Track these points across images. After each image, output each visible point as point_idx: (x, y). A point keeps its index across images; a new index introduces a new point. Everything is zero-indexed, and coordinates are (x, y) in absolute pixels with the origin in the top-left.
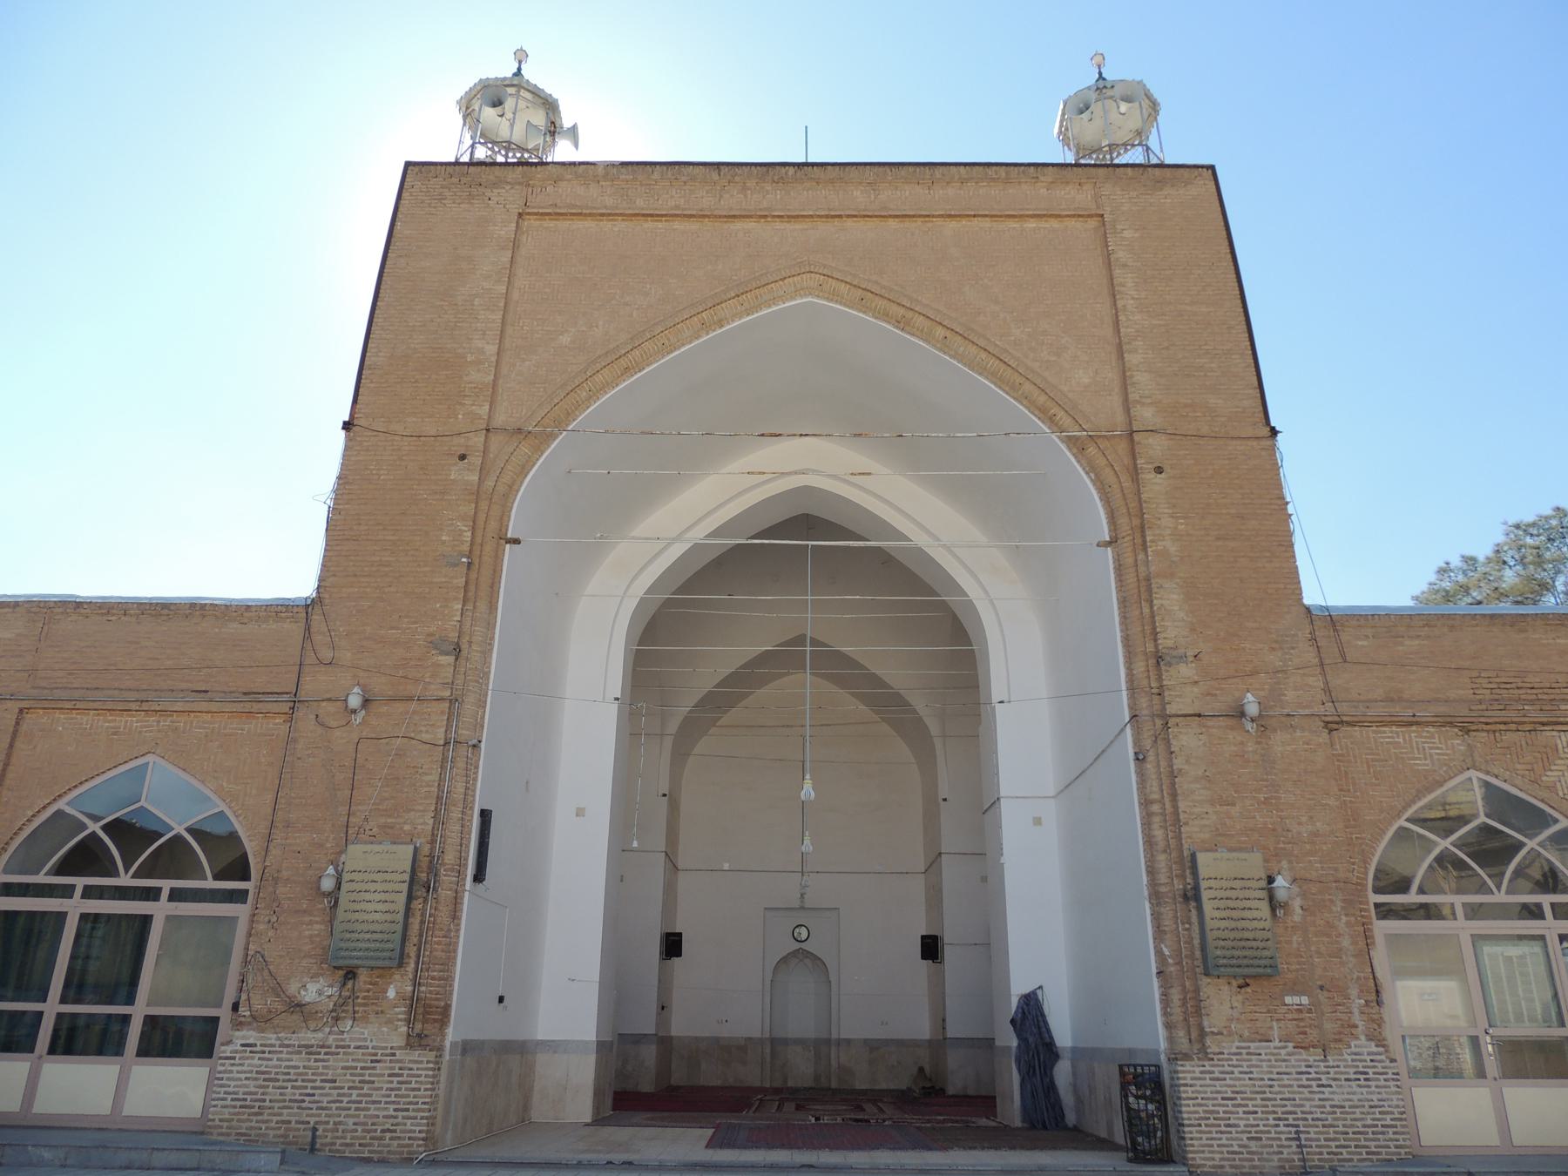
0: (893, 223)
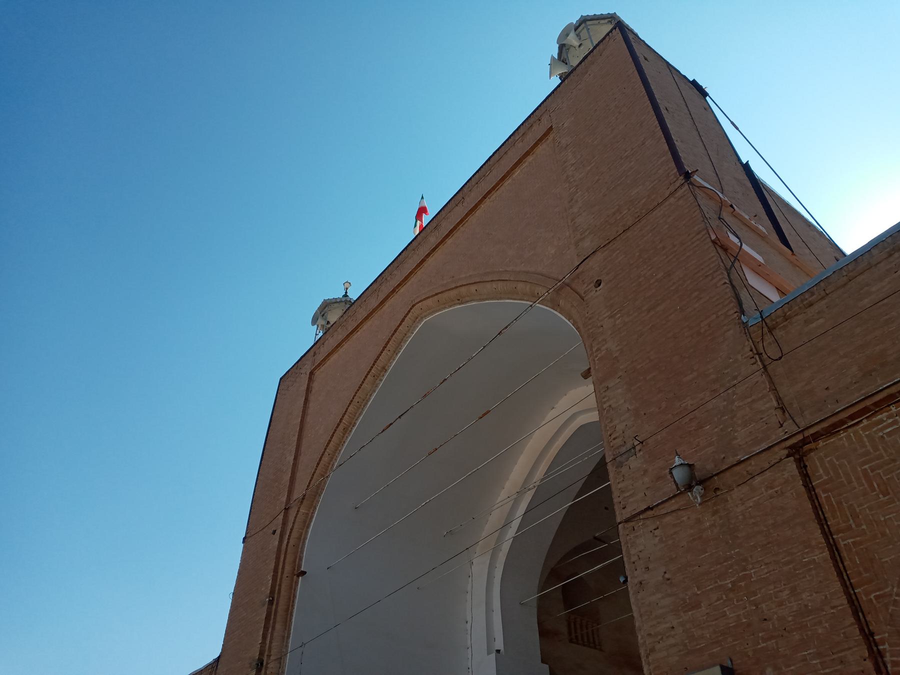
0: (449, 241)
